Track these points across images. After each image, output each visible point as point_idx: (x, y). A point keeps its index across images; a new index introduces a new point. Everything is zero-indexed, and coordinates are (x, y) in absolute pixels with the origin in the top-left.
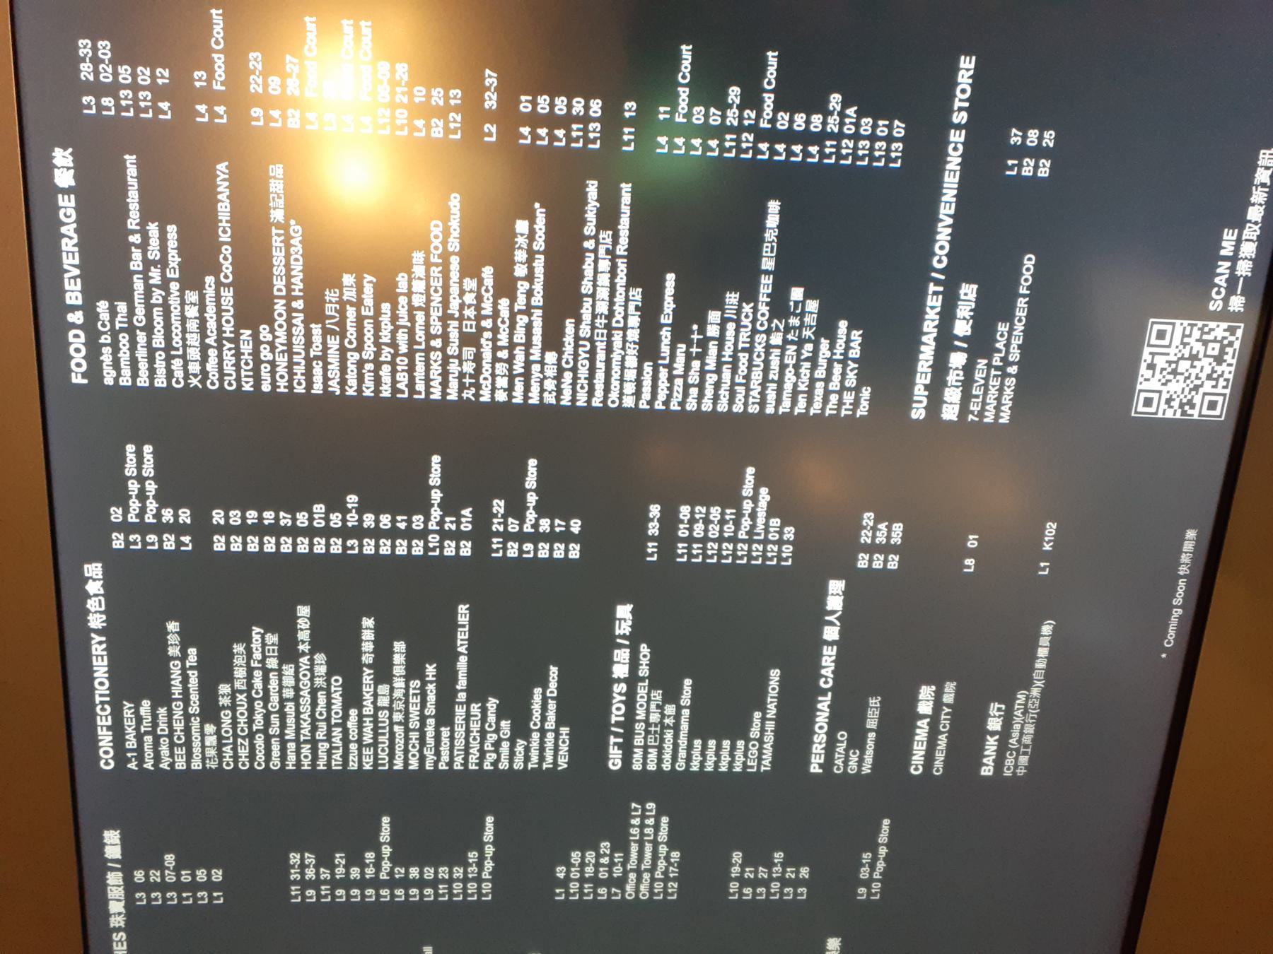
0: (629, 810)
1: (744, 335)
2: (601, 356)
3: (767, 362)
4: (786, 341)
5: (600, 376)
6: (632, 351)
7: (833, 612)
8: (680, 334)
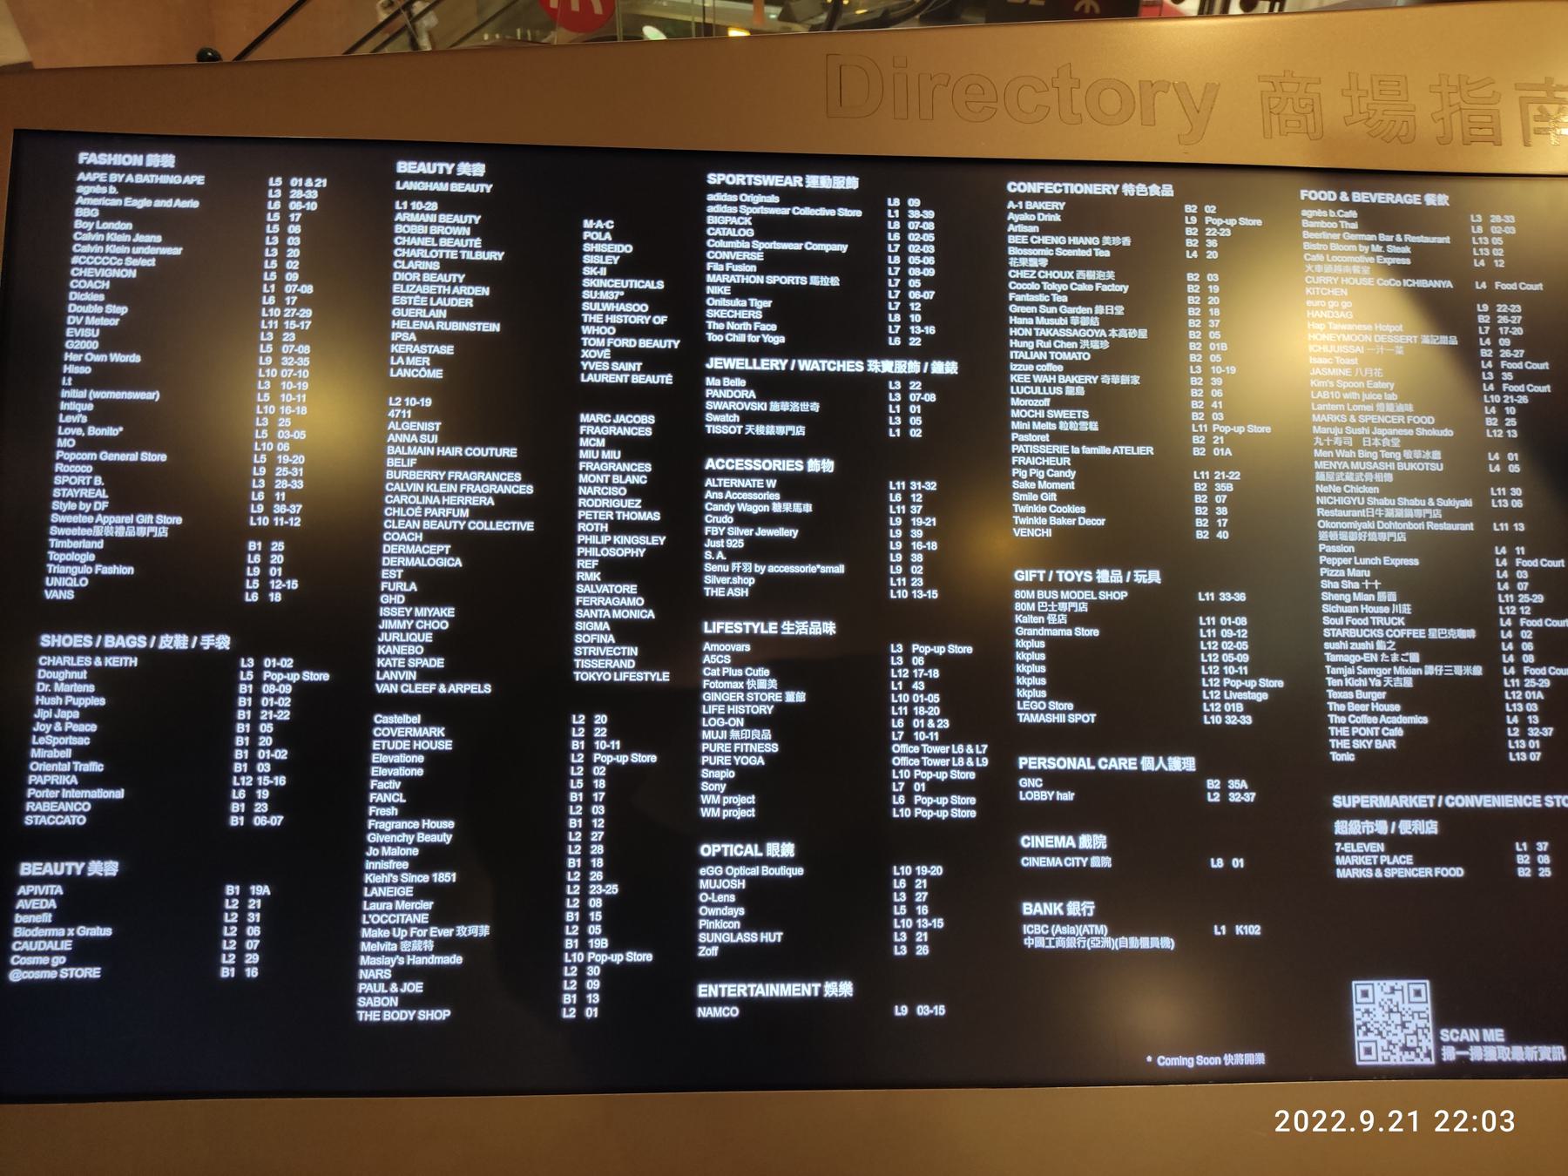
0: (980, 743)
1: (1381, 621)
2: (1356, 513)
3: (1363, 640)
4: (1379, 652)
5: (1341, 513)
6: (1361, 537)
7: (1166, 763)
8: (1377, 572)
